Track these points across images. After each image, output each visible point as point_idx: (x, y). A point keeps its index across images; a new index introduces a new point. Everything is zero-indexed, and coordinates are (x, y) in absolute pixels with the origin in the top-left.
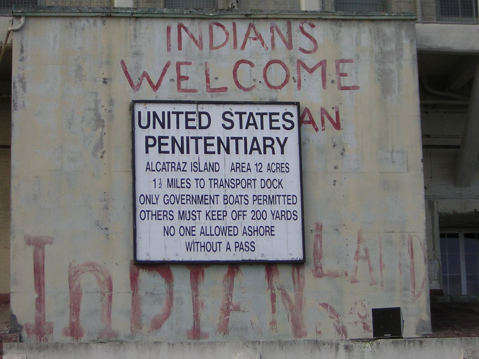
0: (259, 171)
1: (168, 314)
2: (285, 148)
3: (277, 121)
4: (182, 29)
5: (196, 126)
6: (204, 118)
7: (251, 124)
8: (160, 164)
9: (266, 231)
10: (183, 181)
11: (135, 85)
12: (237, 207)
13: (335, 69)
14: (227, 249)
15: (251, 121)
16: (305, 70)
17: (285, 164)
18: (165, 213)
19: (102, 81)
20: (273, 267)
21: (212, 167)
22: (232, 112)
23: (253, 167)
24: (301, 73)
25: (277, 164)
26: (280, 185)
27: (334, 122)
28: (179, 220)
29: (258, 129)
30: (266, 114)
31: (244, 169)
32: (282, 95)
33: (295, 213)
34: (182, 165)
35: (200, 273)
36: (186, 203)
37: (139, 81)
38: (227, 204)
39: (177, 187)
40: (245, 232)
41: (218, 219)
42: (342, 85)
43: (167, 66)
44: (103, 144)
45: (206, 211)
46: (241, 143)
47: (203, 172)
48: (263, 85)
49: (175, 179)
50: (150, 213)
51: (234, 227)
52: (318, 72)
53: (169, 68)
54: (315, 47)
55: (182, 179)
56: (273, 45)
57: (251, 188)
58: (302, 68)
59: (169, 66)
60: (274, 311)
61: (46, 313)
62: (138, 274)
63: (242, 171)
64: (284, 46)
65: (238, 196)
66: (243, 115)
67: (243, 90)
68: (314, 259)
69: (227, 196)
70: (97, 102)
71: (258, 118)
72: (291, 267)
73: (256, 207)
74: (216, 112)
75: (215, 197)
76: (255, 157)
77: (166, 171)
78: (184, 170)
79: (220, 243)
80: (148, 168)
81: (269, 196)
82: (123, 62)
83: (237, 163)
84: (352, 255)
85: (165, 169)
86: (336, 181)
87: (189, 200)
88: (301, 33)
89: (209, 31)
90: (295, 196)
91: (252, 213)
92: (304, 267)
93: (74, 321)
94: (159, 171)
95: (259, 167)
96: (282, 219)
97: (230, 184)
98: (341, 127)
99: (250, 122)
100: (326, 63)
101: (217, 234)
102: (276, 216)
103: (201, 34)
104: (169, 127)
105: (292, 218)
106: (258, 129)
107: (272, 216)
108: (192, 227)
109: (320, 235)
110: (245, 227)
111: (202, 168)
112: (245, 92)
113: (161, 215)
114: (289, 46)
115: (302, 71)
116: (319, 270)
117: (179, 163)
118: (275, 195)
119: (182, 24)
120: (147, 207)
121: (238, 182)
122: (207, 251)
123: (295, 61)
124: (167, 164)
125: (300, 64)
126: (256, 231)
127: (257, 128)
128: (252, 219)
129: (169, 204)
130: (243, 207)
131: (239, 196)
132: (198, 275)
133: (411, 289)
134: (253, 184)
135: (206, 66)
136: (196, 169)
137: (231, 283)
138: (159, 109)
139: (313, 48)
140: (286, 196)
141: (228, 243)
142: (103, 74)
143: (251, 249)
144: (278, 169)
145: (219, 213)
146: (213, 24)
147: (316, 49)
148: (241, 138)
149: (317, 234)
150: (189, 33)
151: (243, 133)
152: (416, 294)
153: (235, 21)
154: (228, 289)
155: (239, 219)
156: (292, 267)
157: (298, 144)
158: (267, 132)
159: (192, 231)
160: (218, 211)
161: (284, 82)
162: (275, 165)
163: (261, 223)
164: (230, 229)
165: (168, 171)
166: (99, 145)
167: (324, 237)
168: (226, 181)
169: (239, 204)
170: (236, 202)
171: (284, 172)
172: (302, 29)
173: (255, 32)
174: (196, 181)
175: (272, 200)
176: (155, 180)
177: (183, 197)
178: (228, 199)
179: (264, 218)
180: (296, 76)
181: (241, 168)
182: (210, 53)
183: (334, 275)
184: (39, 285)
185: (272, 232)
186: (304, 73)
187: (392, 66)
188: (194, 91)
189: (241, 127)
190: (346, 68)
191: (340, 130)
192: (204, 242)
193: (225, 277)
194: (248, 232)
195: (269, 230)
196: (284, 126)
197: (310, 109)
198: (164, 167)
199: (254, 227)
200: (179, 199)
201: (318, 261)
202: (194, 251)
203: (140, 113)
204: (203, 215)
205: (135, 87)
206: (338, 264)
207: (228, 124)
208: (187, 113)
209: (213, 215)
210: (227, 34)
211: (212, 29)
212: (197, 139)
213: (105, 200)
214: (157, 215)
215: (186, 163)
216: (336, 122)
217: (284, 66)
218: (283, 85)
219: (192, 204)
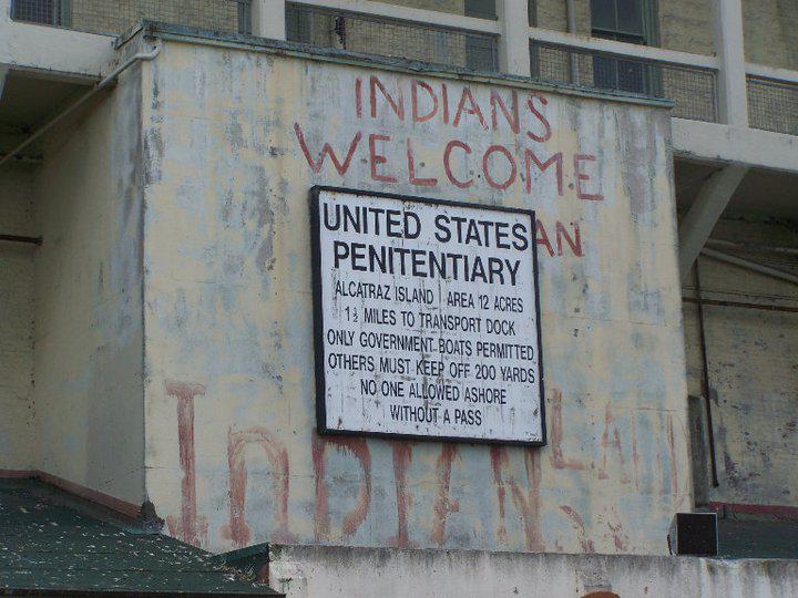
1: (363, 514)
3: (507, 235)
12: (456, 358)
15: (473, 234)
18: (363, 360)
21: (422, 296)
34: (384, 290)
43: (358, 138)
46: (461, 262)
52: (552, 168)
56: (495, 124)
60: (503, 515)
61: (198, 501)
70: (263, 182)
71: (481, 229)
74: (428, 214)
76: (478, 287)
80: (338, 290)
82: (297, 126)
84: (599, 438)
93: (237, 515)
95: (484, 302)
102: (509, 375)
104: (365, 232)
114: (516, 128)
120: (338, 348)
121: (459, 321)
123: (523, 149)
127: (480, 244)
133: (673, 493)
134: (476, 325)
138: (352, 202)
147: (549, 135)
148: (460, 257)
152: (679, 499)
153: (445, 83)
158: (493, 251)
163: (489, 384)
164: (449, 390)
166: (267, 249)
167: (564, 410)
172: (530, 103)
175: (501, 351)
176: (348, 309)
183: (577, 467)
184: (187, 459)
186: (535, 169)
187: (643, 171)
194: (472, 396)
196: (514, 243)
200: (380, 340)
203: (326, 205)
204: (413, 365)
205: (316, 166)
207: (443, 235)
208: (389, 212)
210: (435, 100)
212: (403, 252)
214: (350, 363)
217: (510, 158)
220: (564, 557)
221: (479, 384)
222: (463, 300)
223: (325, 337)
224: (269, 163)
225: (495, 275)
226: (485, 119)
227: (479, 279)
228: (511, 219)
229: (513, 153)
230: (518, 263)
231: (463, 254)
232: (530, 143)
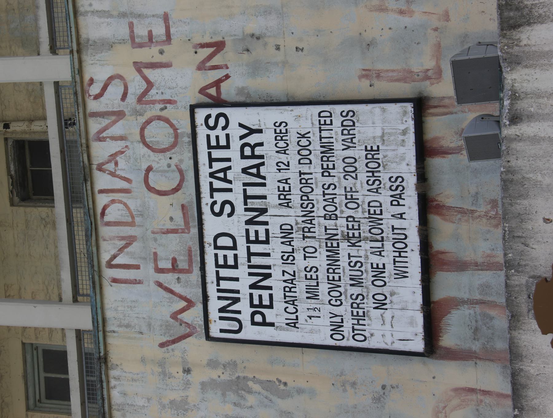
0: (288, 166)
3: (217, 137)
4: (114, 262)
6: (222, 242)
8: (287, 307)
9: (373, 158)
10: (309, 277)
11: (189, 331)
13: (143, 48)
14: (401, 218)
15: (221, 175)
16: (150, 93)
19: (187, 375)
20: (428, 145)
24: (154, 98)
25: (276, 140)
26: (306, 136)
27: (215, 50)
29: (231, 166)
32: (185, 127)
33: (344, 114)
34: (287, 277)
35: (440, 256)
36: (339, 275)
37: (183, 325)
38: (336, 215)
39: (318, 285)
40: (375, 190)
41: (359, 229)
42: (164, 38)
43: (160, 285)
45: (348, 246)
46: (251, 191)
47: (295, 248)
48: (174, 153)
49: (307, 289)
50: (356, 327)
51: (369, 206)
52: (150, 73)
53: (163, 283)
54: (118, 78)
55: (306, 279)
56: (122, 138)
58: (147, 98)
59: (162, 283)
63: (290, 191)
64: (121, 122)
65: (324, 198)
66: (214, 187)
68: (414, 81)
69: (325, 215)
71: (217, 166)
73: (338, 172)
75: (328, 231)
77: (296, 300)
78: (293, 274)
80: (293, 324)
81: (322, 153)
82: (162, 345)
83: (279, 199)
84: (406, 20)
85: (293, 301)
86: (297, 48)
87: (334, 270)
88: (102, 99)
89: (112, 226)
90: (319, 114)
91: (347, 179)
94: (297, 311)
95: (283, 166)
97: (308, 209)
99: (223, 177)
100: (137, 62)
101: (380, 231)
103: (117, 237)
104: (238, 292)
105: (352, 118)
106: (231, 166)
107: (351, 149)
108: (372, 267)
109: (377, 72)
110: (369, 190)
111: (289, 249)
113: (358, 312)
114: (120, 115)
115: (152, 98)
116: (430, 73)
117: (285, 281)
119: (107, 262)
121: (305, 196)
122: (406, 249)
123: (139, 107)
125: (142, 100)
126: (373, 174)
127: (229, 168)
129: (342, 300)
131: (324, 196)
134: (306, 177)
135: (157, 233)
136: (291, 258)
137: (456, 212)
138: (215, 305)
139: (119, 80)
140: (320, 128)
141: (392, 216)
142: (177, 373)
143: (400, 182)
144: (284, 138)
145: (350, 227)
146: (103, 220)
147: (120, 77)
148: (245, 191)
150: (117, 254)
151: (238, 187)
154: (463, 216)
155: (358, 199)
156: (427, 117)
157: (246, 108)
158: (234, 153)
160: (348, 228)
161: (167, 123)
162: (278, 143)
163: (361, 165)
164: (372, 212)
165: (296, 297)
167: (379, 66)
169: (336, 198)
170: (333, 202)
171: (286, 130)
172: (97, 97)
173: (107, 163)
174: (307, 259)
176: (310, 317)
177: (331, 278)
178: (330, 213)
179: (353, 160)
180: (159, 106)
181: (285, 193)
182: (139, 226)
188: (190, 251)
189: (230, 190)
190: (141, 31)
192: (394, 251)
193: (446, 220)
194: (375, 186)
196: (224, 128)
197: (201, 87)
199: (367, 177)
201: (416, 76)
202: (407, 267)
203: (222, 331)
206: (420, 43)
207: (228, 208)
210: (113, 201)
211: (109, 222)
212: (250, 254)
217: (148, 122)
218: (172, 125)
219: (339, 265)
220: (515, 333)
221: (363, 176)
222: (284, 191)
223: (338, 343)
224: (197, 377)
225: (257, 153)
226: (118, 149)
227: (263, 171)
228: (202, 132)
229: (142, 120)
230: (241, 125)
232: (131, 99)
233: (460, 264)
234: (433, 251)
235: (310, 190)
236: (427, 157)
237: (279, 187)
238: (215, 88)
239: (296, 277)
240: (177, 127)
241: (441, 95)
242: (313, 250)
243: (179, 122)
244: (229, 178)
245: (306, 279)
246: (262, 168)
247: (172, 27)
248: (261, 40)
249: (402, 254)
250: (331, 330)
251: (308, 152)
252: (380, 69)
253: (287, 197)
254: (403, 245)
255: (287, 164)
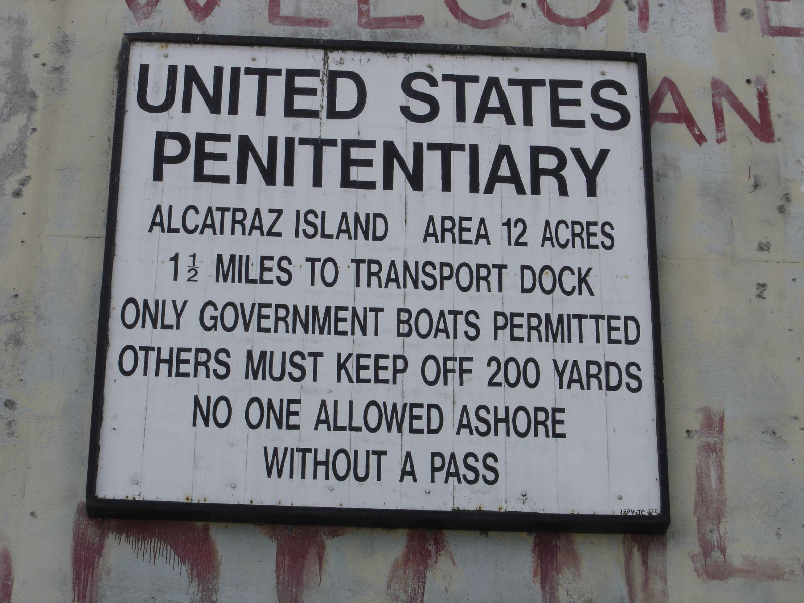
0: (517, 243)
2: (600, 179)
3: (576, 103)
5: (317, 108)
7: (504, 180)
8: (197, 212)
9: (537, 423)
10: (268, 264)
12: (440, 346)
14: (404, 473)
15: (494, 102)
17: (600, 224)
18: (203, 357)
20: (561, 543)
22: (433, 74)
23: (496, 231)
25: (574, 223)
26: (584, 285)
28: (247, 377)
30: (540, 83)
31: (466, 236)
33: (633, 370)
34: (267, 219)
35: (313, 551)
36: (273, 330)
38: (408, 334)
39: (248, 281)
41: (378, 381)
42: (775, 23)
44: (25, 156)
45: (339, 355)
46: (460, 162)
48: (534, 14)
49: (241, 257)
50: (153, 355)
55: (263, 259)
57: (489, 290)
62: (101, 547)
63: (462, 241)
65: (446, 313)
67: (471, 25)
68: (699, 521)
69: (408, 311)
70: (19, 45)
71: (514, 96)
72: (621, 545)
73: (504, 348)
75: (371, 315)
78: (274, 230)
79: (380, 454)
81: (548, 316)
83: (444, 218)
85: (212, 226)
86: (764, 285)
87: (284, 319)
91: (489, 365)
92: (664, 545)
94: (192, 232)
95: (515, 232)
96: (589, 388)
97: (422, 277)
98: (777, 134)
104: (233, 109)
105: (623, 385)
107: (557, 378)
108: (290, 402)
109: (717, 447)
110: (465, 408)
111: (331, 227)
112: (476, 29)
116: (716, 555)
117: (258, 212)
118: (569, 315)
120: (144, 335)
124: (220, 213)
126: (501, 420)
127: (510, 120)
128: (491, 384)
129: (215, 330)
130: (462, 347)
131: (450, 312)
132: (303, 557)
134: (494, 278)
136: (310, 231)
140: (602, 317)
141: (408, 455)
143: (484, 477)
144: (578, 240)
145: (382, 363)
148: (461, 148)
149: (708, 444)
151: (468, 133)
155: (446, 383)
156: (624, 543)
159: (290, 413)
160: (378, 357)
162: (567, 227)
163: (521, 396)
164: (416, 411)
165: (222, 232)
167: (730, 453)
168: (406, 267)
169: (448, 337)
170: (438, 330)
171: (596, 247)
174: (310, 263)
176: (175, 259)
177: (265, 311)
178: (412, 322)
181: (456, 231)
185: (558, 426)
188: (320, 22)
191: (770, 144)
192: (328, 451)
193: (395, 567)
194: (475, 422)
195: (547, 419)
196: (596, 118)
198: (209, 222)
199: (496, 408)
201: (708, 528)
203: (144, 69)
204: (327, 365)
206: (778, 538)
207: (421, 108)
208: (292, 74)
209: (360, 368)
212: (318, 145)
213: (14, 318)
215: (280, 212)
216: (759, 121)
219: (294, 331)
227: (505, 190)
230: (603, 155)
231: (467, 142)
233: (295, 591)
234: (324, 537)
235: (465, 284)
236: (535, 540)
237: (470, 219)
238: (676, 111)
239: (266, 238)
240: (592, 26)
241: (670, 577)
242: (329, 277)
243: (601, 30)
244: (489, 117)
245: (263, 259)
246: (511, 187)
247: (797, 41)
248: (778, 214)
249: (321, 469)
250: (146, 302)
251: (548, 287)
252: (724, 453)
253: (448, 236)
254: (341, 471)
255: (520, 241)
